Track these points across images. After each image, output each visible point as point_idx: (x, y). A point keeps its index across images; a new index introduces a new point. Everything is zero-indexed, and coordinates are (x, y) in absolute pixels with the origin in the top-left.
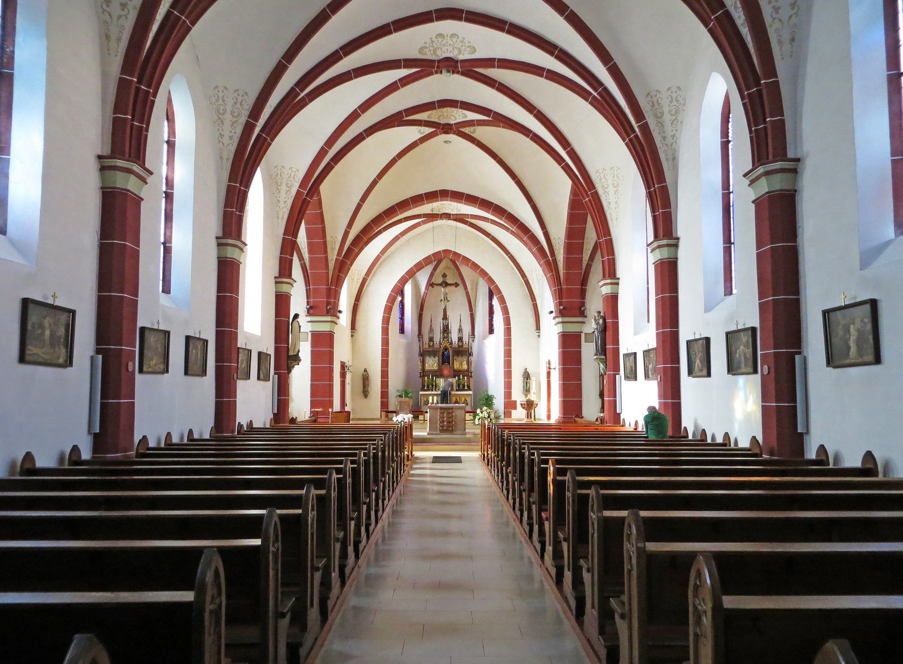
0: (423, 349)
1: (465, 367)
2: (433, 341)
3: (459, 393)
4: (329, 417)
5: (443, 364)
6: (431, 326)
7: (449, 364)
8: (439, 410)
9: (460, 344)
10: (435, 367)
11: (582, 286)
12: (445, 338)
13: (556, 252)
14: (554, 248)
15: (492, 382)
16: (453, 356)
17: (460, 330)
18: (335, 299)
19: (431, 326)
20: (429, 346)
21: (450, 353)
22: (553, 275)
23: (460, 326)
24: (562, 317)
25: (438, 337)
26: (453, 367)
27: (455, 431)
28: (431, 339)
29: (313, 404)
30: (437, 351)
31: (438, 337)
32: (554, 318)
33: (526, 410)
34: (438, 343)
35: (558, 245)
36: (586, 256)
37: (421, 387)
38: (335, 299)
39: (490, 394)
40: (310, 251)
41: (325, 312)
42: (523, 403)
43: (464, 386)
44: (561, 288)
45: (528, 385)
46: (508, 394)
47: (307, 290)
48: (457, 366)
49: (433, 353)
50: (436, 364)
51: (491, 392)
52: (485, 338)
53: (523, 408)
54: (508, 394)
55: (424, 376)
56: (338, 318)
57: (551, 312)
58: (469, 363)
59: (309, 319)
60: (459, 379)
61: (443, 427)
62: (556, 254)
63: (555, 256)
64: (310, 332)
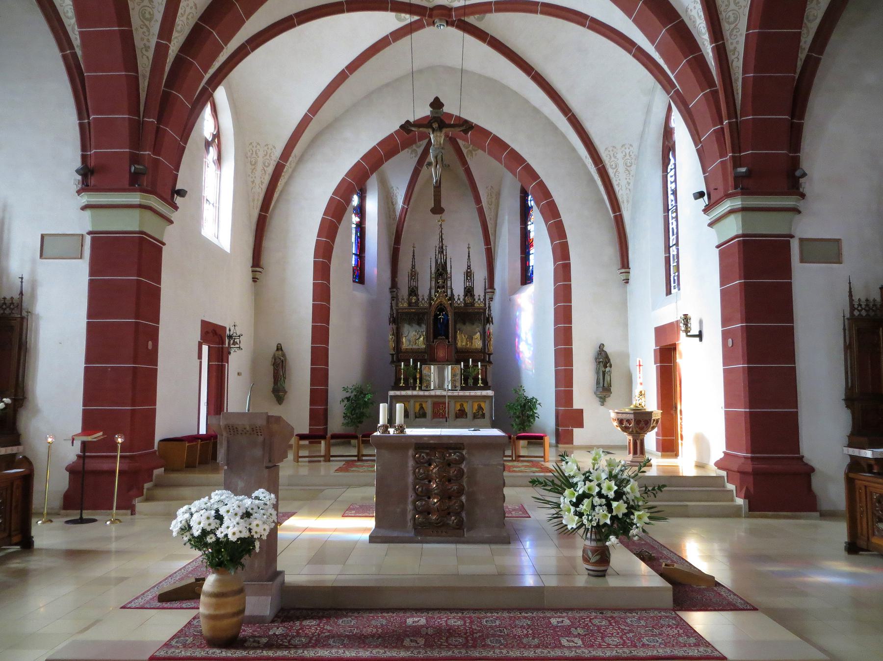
0: (397, 310)
1: (478, 343)
2: (417, 295)
3: (467, 393)
4: (116, 457)
5: (435, 337)
6: (413, 266)
7: (447, 338)
8: (411, 452)
9: (469, 300)
10: (421, 343)
11: (792, 119)
12: (439, 287)
13: (726, 27)
14: (723, 16)
15: (530, 373)
16: (455, 323)
17: (469, 275)
18: (156, 150)
19: (413, 266)
20: (410, 304)
21: (450, 317)
22: (715, 93)
23: (469, 267)
24: (743, 194)
25: (425, 286)
26: (456, 344)
27: (469, 529)
28: (413, 291)
29: (90, 422)
30: (424, 314)
31: (425, 286)
32: (707, 210)
33: (630, 434)
34: (426, 298)
35: (732, 6)
36: (807, 39)
37: (393, 384)
38: (156, 150)
39: (530, 397)
40: (82, 17)
41: (126, 182)
42: (624, 416)
43: (476, 380)
44: (737, 122)
45: (607, 378)
46: (564, 395)
47: (82, 126)
48: (462, 342)
49: (414, 316)
50: (422, 339)
51: (530, 391)
52: (515, 291)
53: (625, 429)
54: (564, 395)
55: (399, 361)
56: (176, 208)
57: (700, 195)
58: (485, 337)
59: (85, 199)
60: (467, 366)
61: (426, 511)
62: (727, 34)
63: (723, 39)
64: (90, 233)
